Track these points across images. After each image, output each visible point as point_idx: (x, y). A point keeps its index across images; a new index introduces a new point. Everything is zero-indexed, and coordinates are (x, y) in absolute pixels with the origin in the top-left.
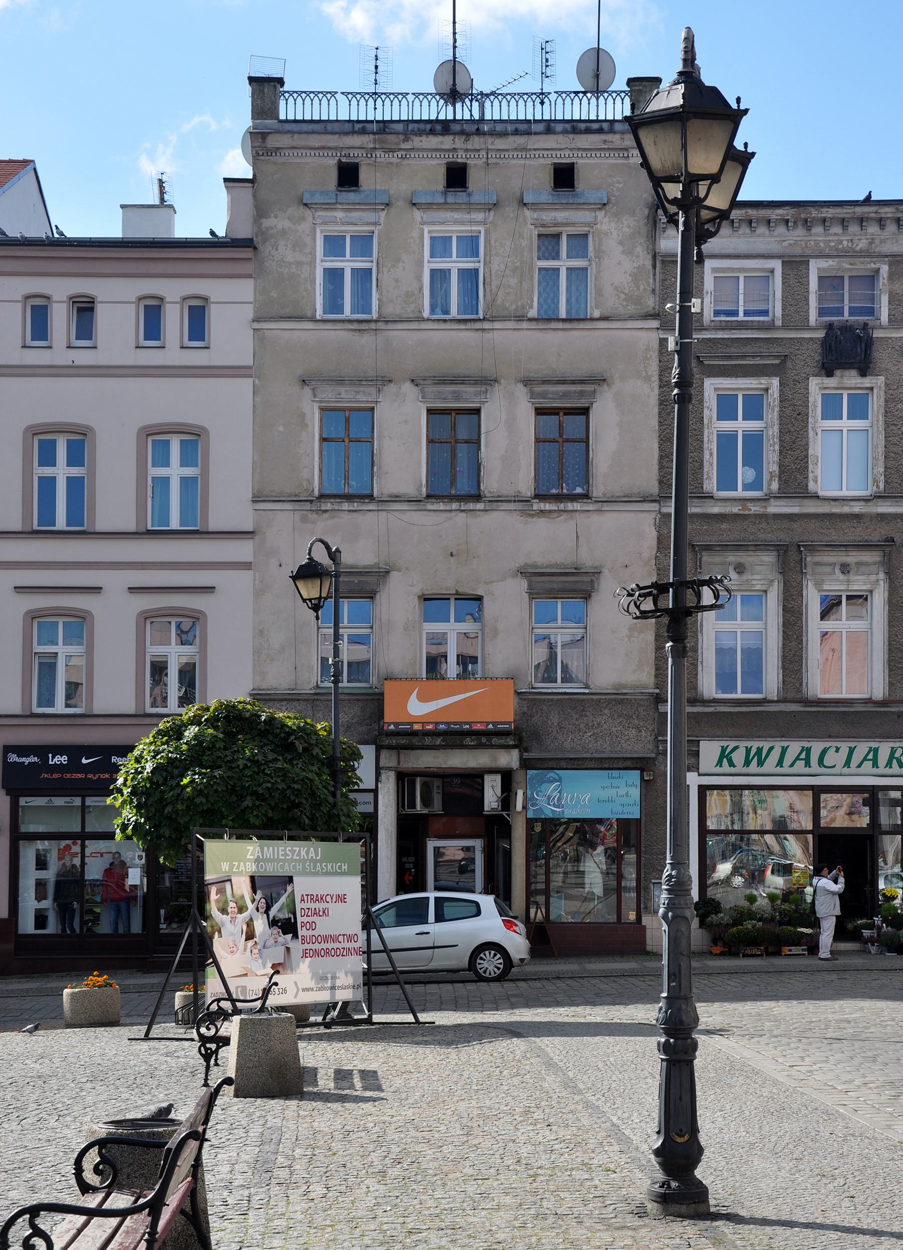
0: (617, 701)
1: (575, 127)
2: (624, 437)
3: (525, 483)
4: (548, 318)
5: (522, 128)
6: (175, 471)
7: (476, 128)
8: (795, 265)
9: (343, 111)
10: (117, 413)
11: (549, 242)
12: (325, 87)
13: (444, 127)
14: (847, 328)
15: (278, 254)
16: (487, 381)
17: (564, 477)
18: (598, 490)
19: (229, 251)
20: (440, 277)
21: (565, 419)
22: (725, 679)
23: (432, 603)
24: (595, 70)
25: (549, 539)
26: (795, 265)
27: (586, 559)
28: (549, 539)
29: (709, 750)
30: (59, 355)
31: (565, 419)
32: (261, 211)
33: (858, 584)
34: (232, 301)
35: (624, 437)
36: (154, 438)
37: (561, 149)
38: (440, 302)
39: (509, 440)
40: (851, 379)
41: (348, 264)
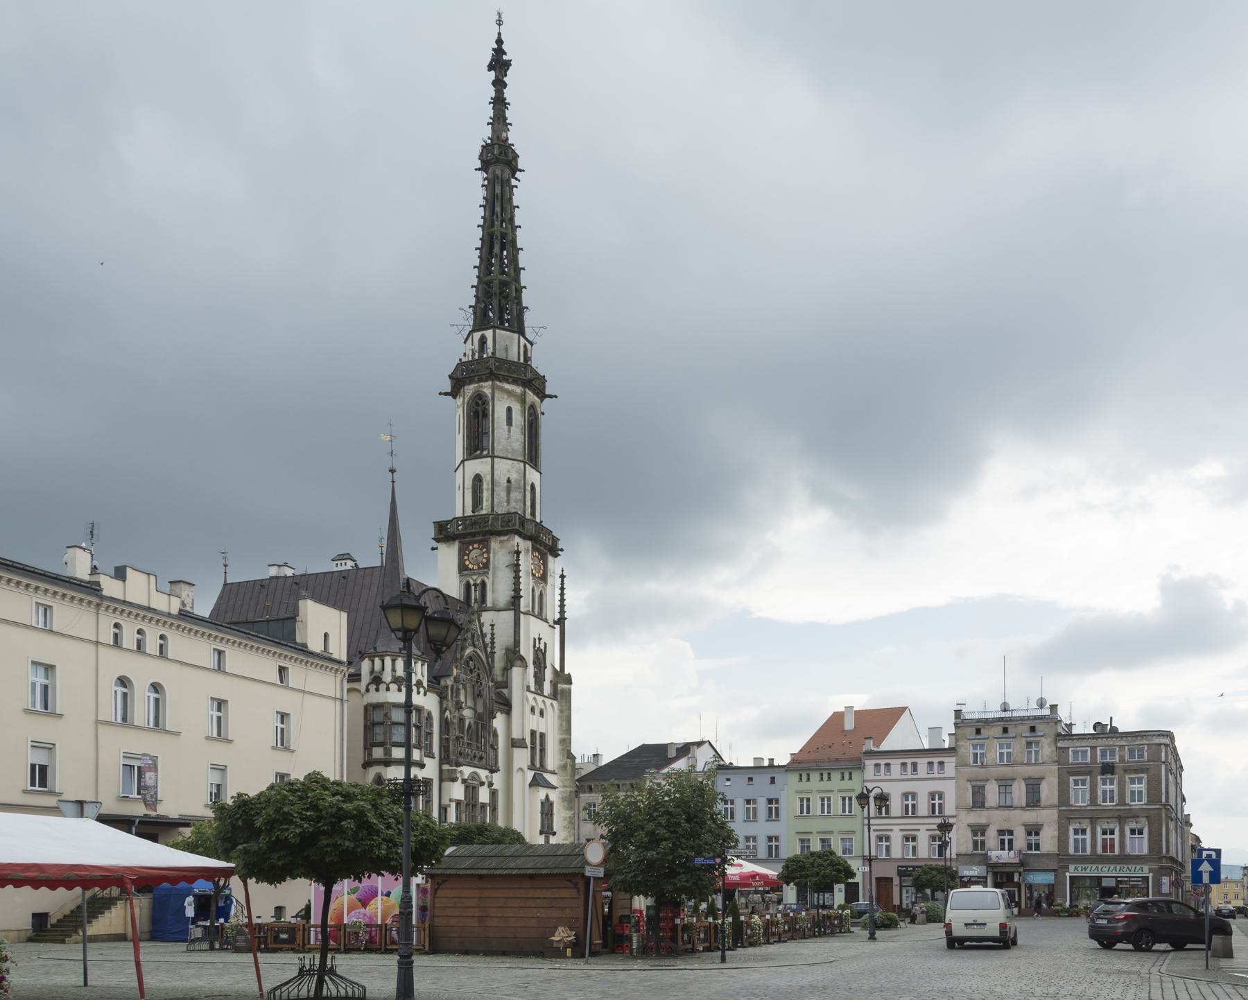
0: (1048, 855)
1: (1036, 718)
2: (1048, 791)
3: (1024, 803)
4: (1027, 764)
5: (1022, 719)
6: (910, 802)
7: (1011, 720)
8: (1093, 748)
9: (977, 716)
10: (922, 790)
11: (1029, 744)
12: (973, 711)
13: (1001, 719)
14: (1108, 764)
15: (961, 751)
16: (1014, 780)
17: (1033, 801)
18: (1043, 804)
19: (952, 751)
20: (1001, 754)
21: (1033, 787)
22: (1076, 849)
23: (1001, 832)
24: (1041, 704)
25: (1030, 816)
26: (1093, 748)
27: (1040, 821)
28: (1030, 816)
29: (1072, 867)
30: (910, 776)
31: (1033, 787)
32: (957, 741)
33: (1111, 826)
34: (950, 762)
35: (1048, 791)
36: (932, 795)
37: (1032, 723)
38: (1001, 760)
39: (1019, 792)
40: (1109, 776)
41: (979, 751)
